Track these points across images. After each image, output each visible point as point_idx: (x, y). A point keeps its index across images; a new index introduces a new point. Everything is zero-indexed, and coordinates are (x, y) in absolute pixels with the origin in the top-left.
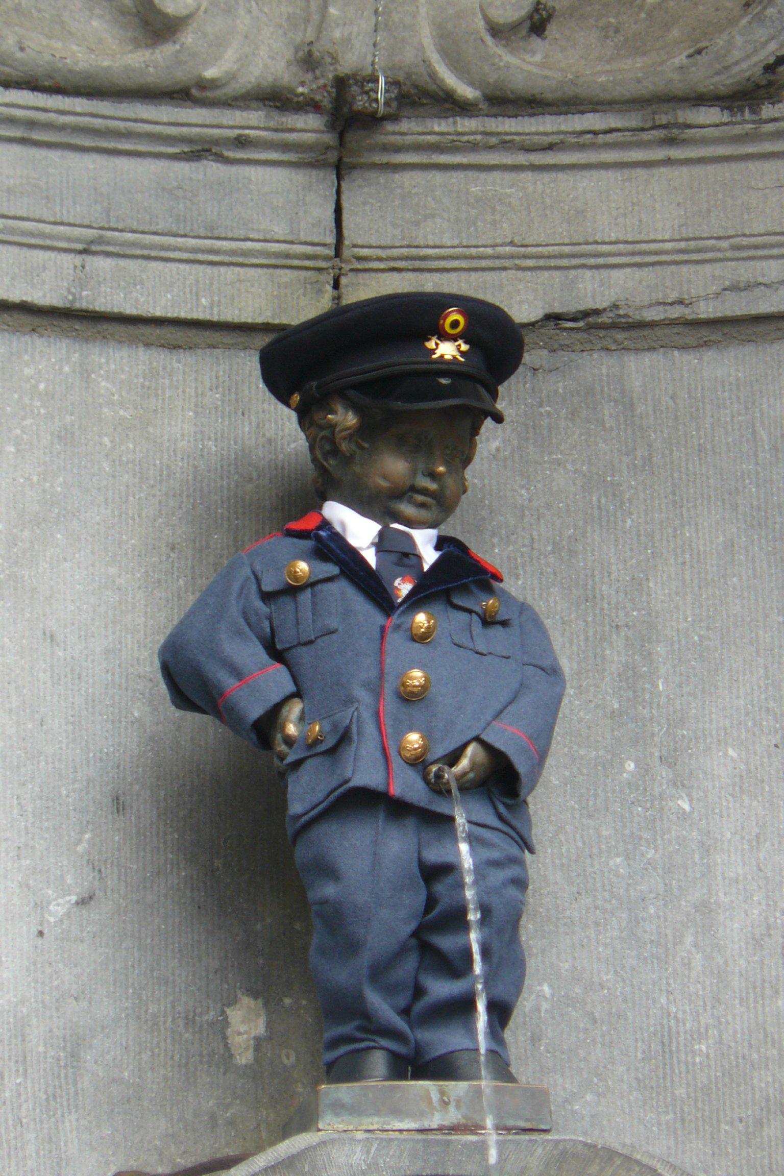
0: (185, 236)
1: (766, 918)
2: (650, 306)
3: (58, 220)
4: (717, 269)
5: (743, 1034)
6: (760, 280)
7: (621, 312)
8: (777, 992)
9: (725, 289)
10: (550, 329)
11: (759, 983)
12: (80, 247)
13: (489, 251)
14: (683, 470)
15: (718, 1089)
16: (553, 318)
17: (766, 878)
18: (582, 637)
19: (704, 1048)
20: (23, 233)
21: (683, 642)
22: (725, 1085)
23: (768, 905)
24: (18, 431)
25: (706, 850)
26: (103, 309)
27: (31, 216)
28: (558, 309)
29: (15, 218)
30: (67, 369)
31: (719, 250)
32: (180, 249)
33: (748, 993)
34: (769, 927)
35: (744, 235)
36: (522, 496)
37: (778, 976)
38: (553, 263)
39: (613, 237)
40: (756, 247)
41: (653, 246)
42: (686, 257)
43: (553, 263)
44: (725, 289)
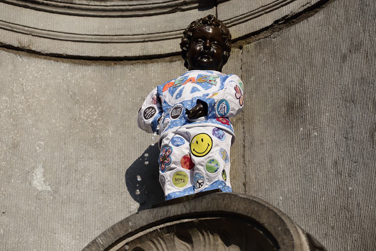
0: (172, 31)
2: (300, 8)
3: (134, 34)
5: (333, 190)
7: (293, 13)
10: (276, 26)
12: (142, 40)
13: (257, 11)
15: (328, 209)
16: (276, 22)
17: (337, 144)
18: (288, 101)
19: (324, 199)
20: (123, 39)
21: (313, 91)
22: (329, 207)
24: (126, 89)
25: (322, 144)
26: (150, 54)
27: (125, 34)
28: (277, 19)
29: (120, 35)
30: (142, 72)
32: (172, 35)
36: (271, 71)
38: (274, 8)
43: (274, 8)
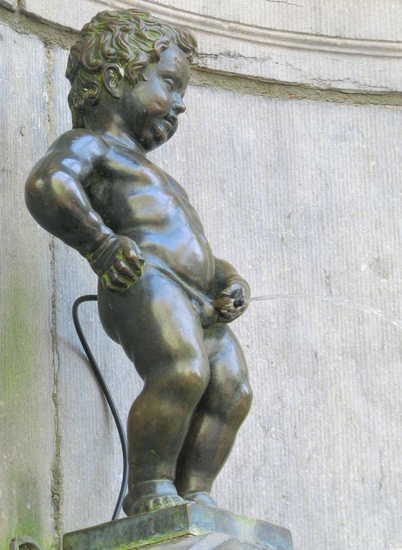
1: (244, 455)
4: (218, 39)
6: (241, 54)
8: (251, 504)
9: (221, 54)
11: (240, 495)
14: (194, 160)
23: (245, 447)
31: (222, 28)
33: (234, 502)
34: (245, 462)
35: (238, 23)
37: (251, 494)
39: (167, 4)
40: (243, 32)
41: (187, 15)
42: (203, 28)
44: (221, 54)
